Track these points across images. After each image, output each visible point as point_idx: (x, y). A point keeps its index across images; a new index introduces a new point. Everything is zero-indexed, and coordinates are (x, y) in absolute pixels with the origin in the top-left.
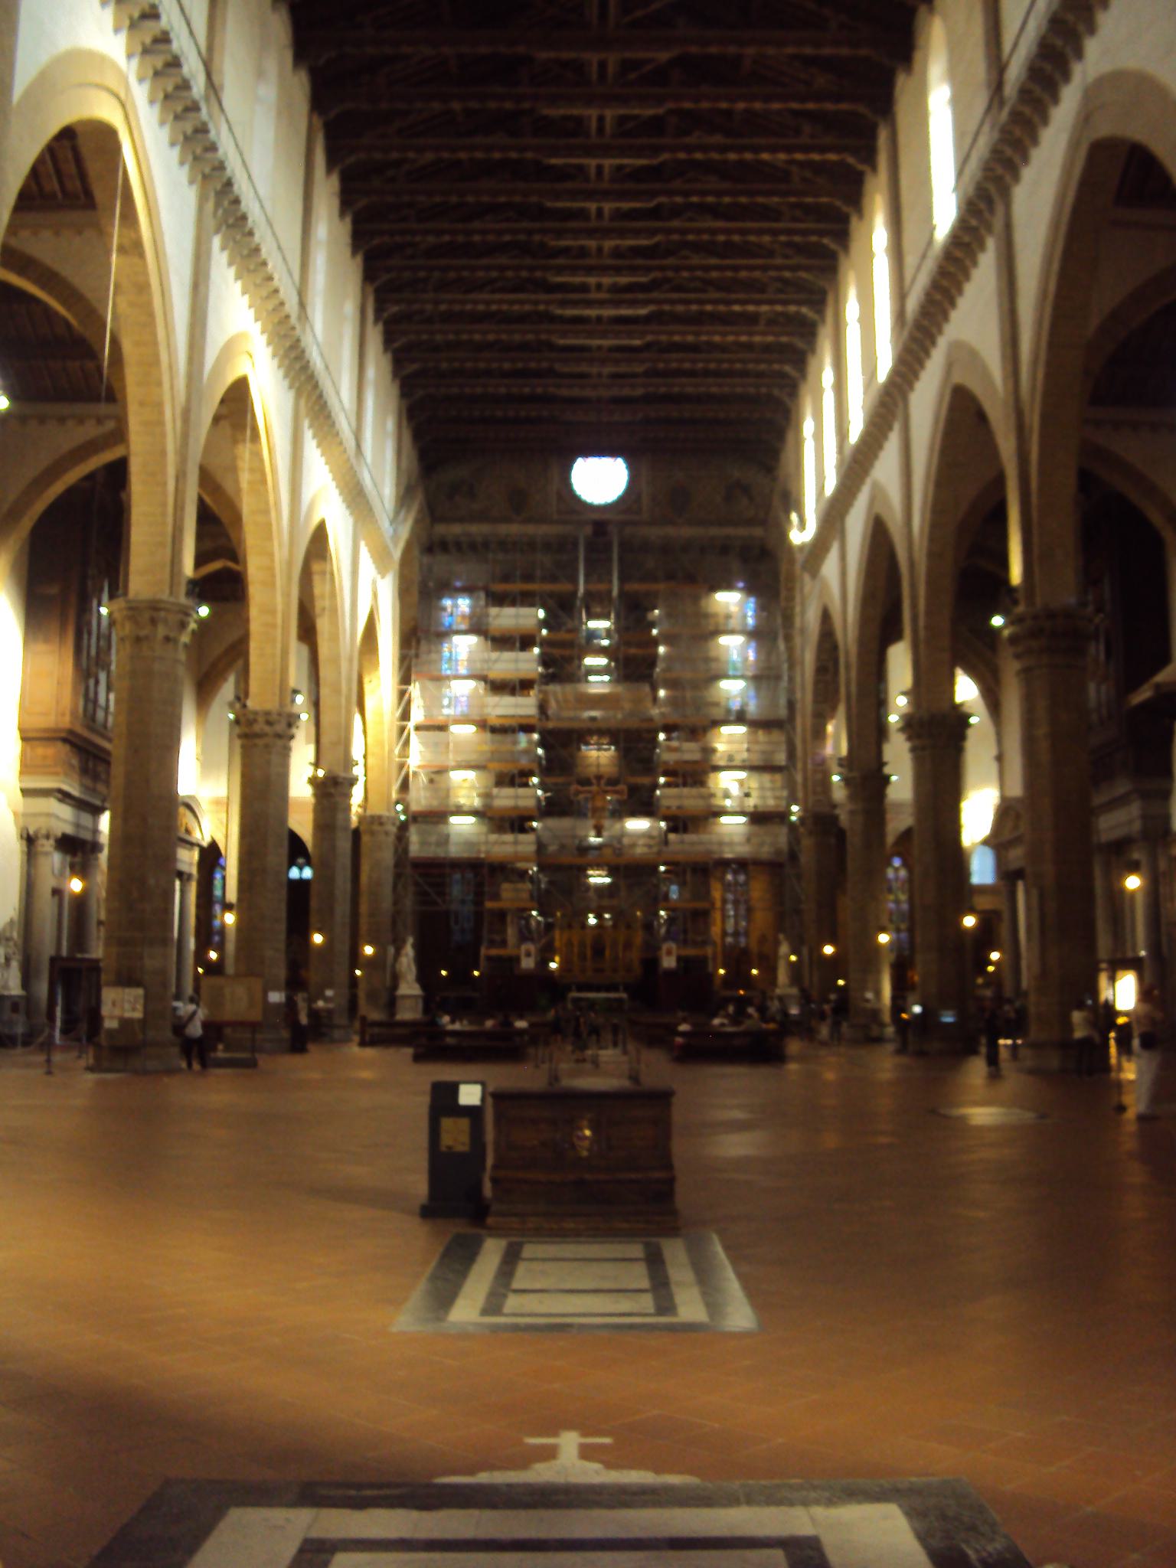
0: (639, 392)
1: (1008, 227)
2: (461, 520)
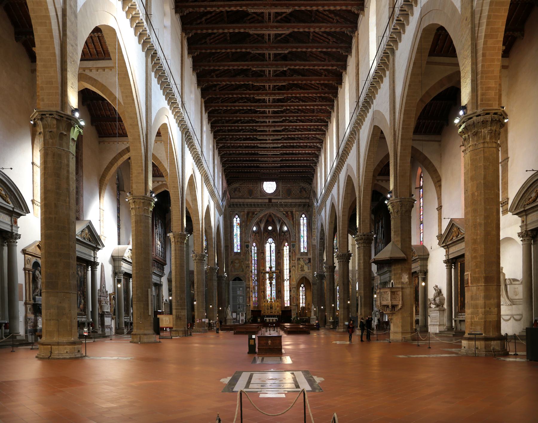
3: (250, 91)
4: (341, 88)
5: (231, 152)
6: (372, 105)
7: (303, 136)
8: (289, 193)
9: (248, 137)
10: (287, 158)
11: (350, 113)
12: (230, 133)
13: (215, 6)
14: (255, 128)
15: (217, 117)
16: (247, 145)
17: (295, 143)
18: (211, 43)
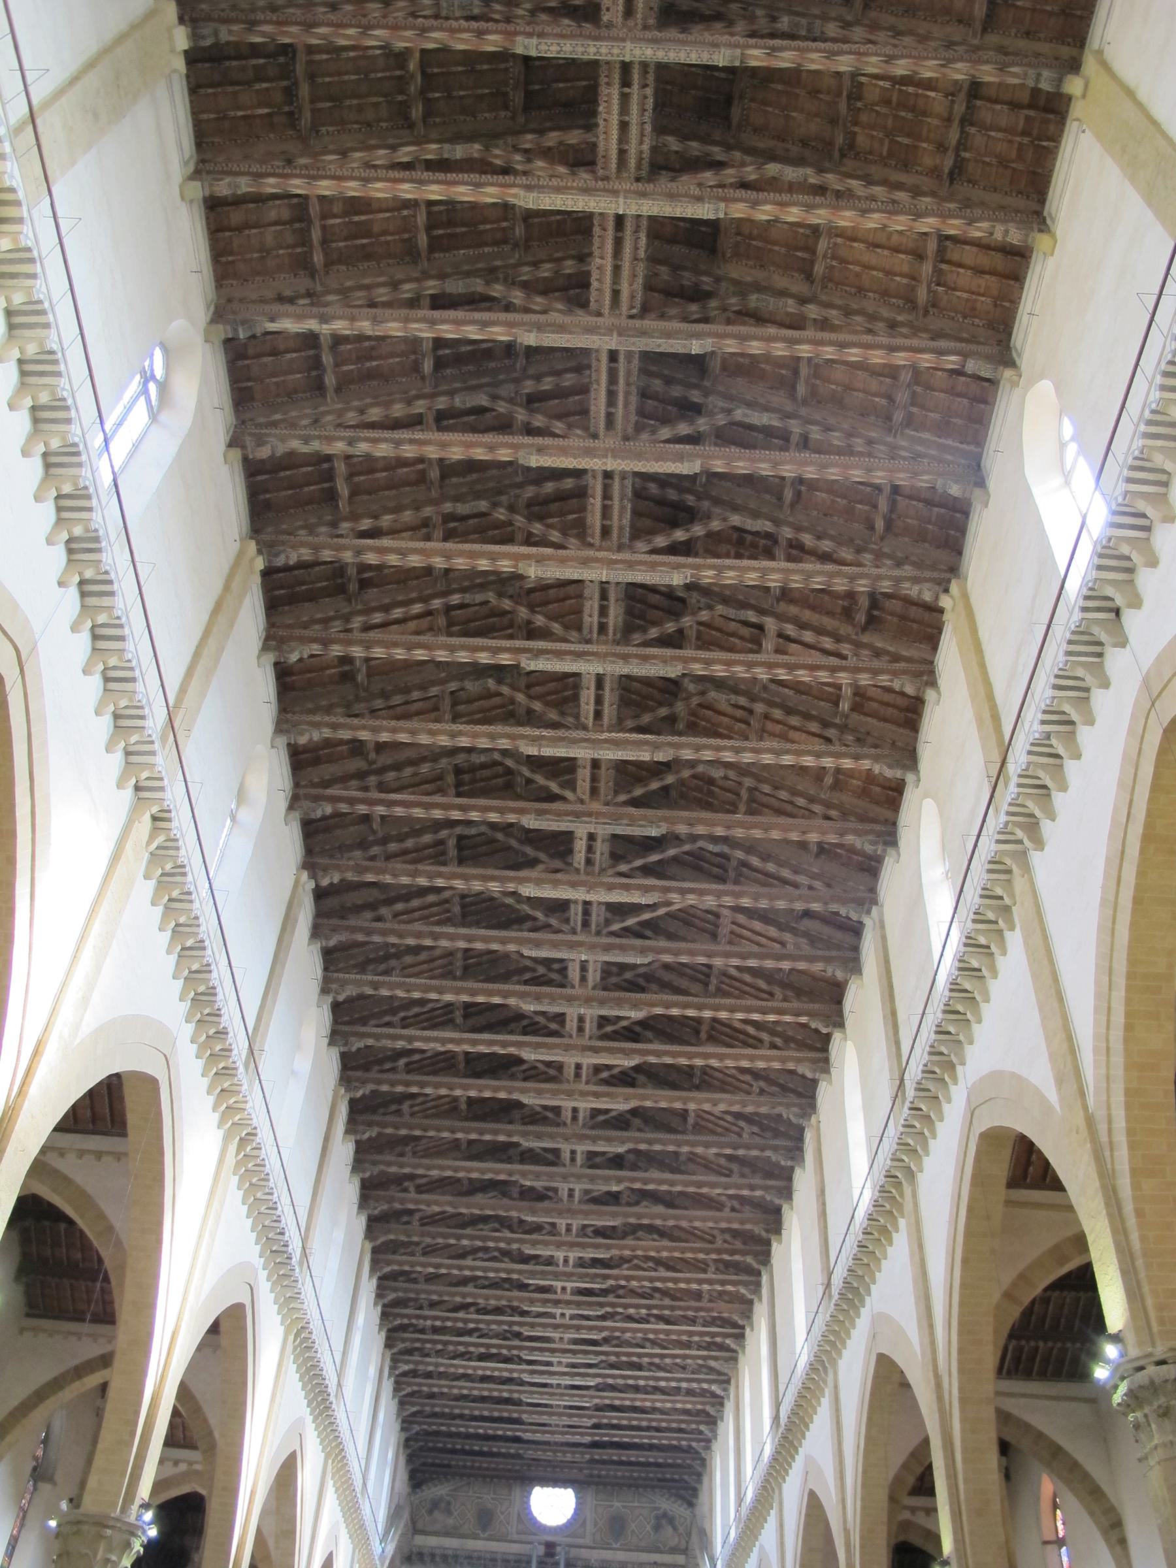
0: (587, 1439)
1: (836, 1387)
2: (435, 1534)
3: (512, 1231)
4: (780, 1242)
5: (435, 1390)
6: (867, 1299)
7: (668, 1361)
8: (617, 1526)
9: (494, 1351)
10: (615, 1422)
11: (807, 1312)
12: (436, 1337)
13: (435, 1040)
14: (516, 1328)
15: (406, 1290)
16: (488, 1373)
17: (642, 1378)
18: (412, 1115)
